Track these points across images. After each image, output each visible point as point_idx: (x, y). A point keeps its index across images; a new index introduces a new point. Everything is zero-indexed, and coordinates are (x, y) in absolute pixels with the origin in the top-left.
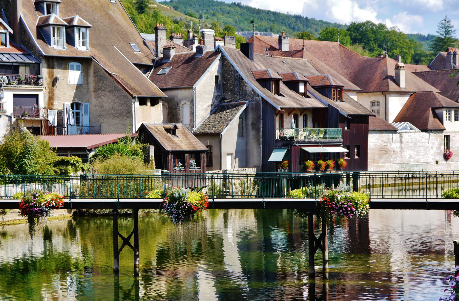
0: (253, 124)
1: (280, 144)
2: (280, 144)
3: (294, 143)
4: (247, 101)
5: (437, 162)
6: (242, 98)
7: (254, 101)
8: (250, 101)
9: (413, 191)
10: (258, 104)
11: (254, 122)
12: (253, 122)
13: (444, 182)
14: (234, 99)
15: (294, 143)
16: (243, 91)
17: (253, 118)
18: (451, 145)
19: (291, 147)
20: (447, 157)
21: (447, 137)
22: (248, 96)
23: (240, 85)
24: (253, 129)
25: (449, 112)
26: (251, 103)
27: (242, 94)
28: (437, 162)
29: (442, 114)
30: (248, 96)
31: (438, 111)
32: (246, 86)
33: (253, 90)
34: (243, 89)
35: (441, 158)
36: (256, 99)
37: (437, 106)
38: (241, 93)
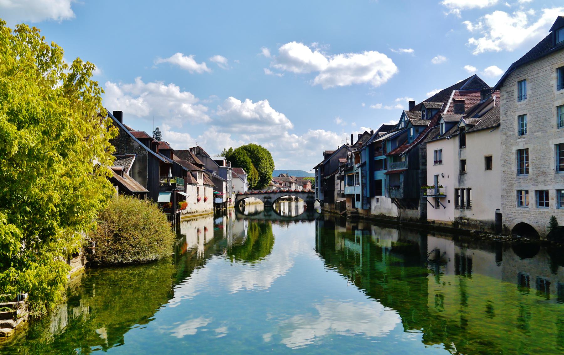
0: (139, 173)
1: (164, 189)
2: (164, 189)
3: (176, 188)
4: (135, 154)
5: (195, 204)
6: (129, 152)
7: (141, 154)
8: (137, 154)
9: (187, 221)
10: (145, 156)
11: (141, 171)
12: (139, 171)
13: (197, 216)
14: (121, 153)
15: (176, 188)
16: (130, 146)
17: (139, 168)
18: (199, 193)
19: (173, 191)
20: (198, 200)
21: (198, 188)
22: (136, 150)
23: (127, 141)
24: (139, 176)
25: (199, 173)
26: (138, 156)
27: (129, 149)
28: (195, 204)
29: (197, 174)
30: (136, 150)
31: (193, 173)
32: (133, 142)
33: (140, 146)
34: (130, 144)
35: (196, 201)
36: (143, 153)
37: (194, 170)
38: (127, 148)
